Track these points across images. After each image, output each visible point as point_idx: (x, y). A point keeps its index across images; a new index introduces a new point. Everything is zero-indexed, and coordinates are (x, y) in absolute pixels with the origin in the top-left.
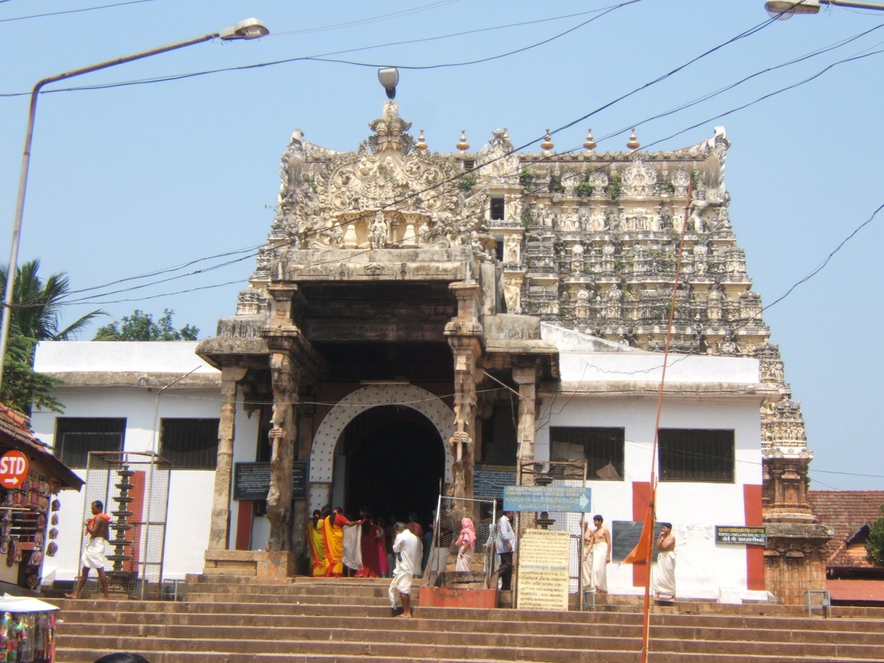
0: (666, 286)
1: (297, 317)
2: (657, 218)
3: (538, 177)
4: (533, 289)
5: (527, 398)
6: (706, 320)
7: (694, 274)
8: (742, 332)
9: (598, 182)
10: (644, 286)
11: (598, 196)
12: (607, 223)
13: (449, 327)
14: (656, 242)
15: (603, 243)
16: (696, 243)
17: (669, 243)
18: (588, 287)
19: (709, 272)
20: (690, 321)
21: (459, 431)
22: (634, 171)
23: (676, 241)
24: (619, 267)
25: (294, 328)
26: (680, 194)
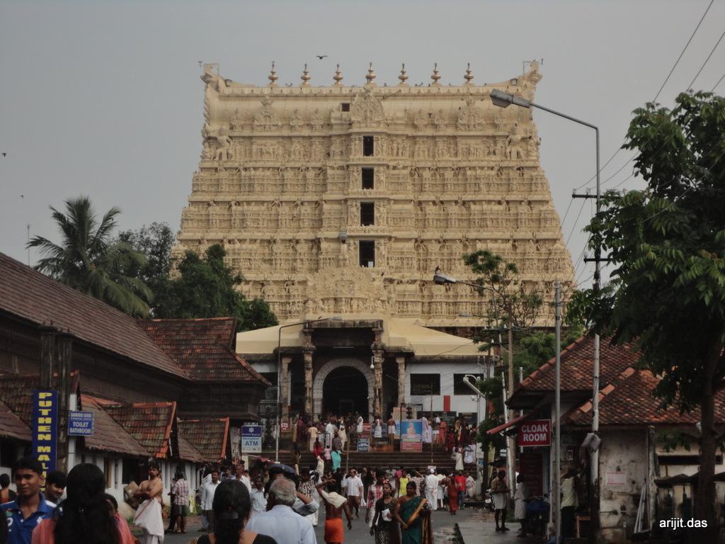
1: (313, 342)
5: (402, 369)
13: (373, 345)
21: (375, 380)
25: (314, 347)
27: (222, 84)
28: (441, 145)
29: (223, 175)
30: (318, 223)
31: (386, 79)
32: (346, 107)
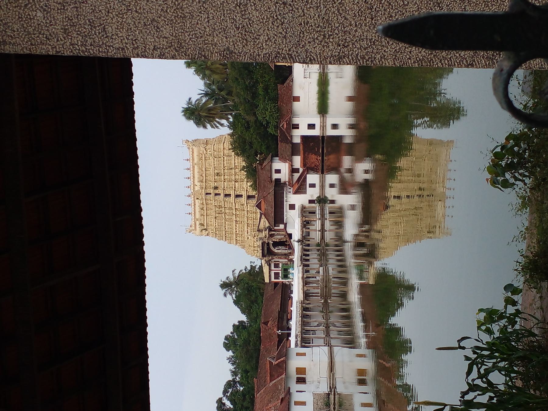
27: (191, 228)
28: (207, 172)
29: (217, 232)
30: (231, 209)
31: (189, 183)
32: (197, 199)
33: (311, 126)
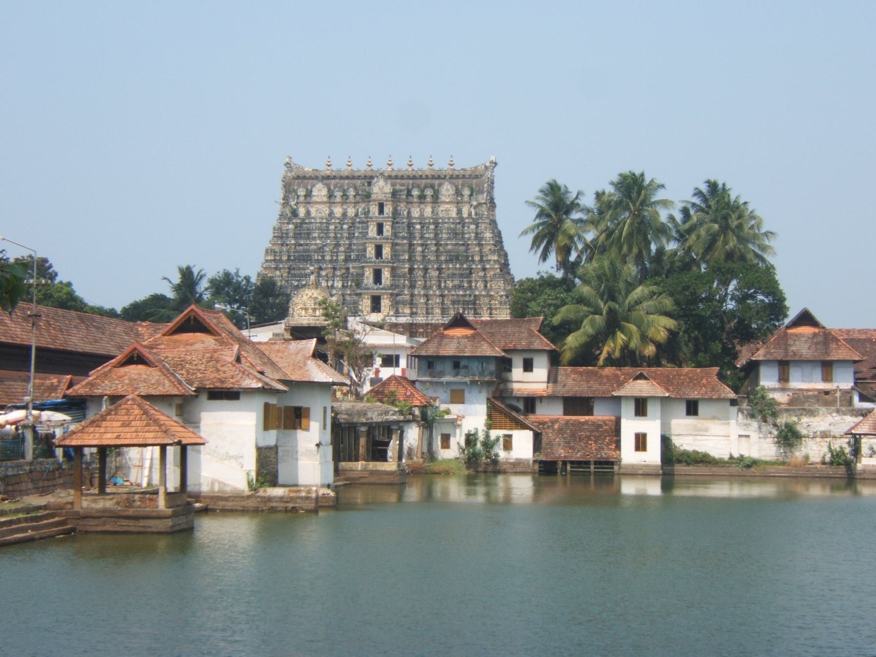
0: (456, 244)
2: (455, 210)
3: (401, 191)
4: (397, 247)
6: (473, 261)
7: (469, 239)
8: (488, 266)
9: (429, 192)
10: (447, 245)
11: (429, 199)
12: (432, 212)
14: (453, 223)
15: (430, 223)
16: (471, 223)
17: (459, 223)
18: (422, 245)
19: (476, 238)
20: (467, 260)
22: (445, 187)
23: (462, 221)
24: (436, 235)
26: (466, 198)
33: (641, 442)
